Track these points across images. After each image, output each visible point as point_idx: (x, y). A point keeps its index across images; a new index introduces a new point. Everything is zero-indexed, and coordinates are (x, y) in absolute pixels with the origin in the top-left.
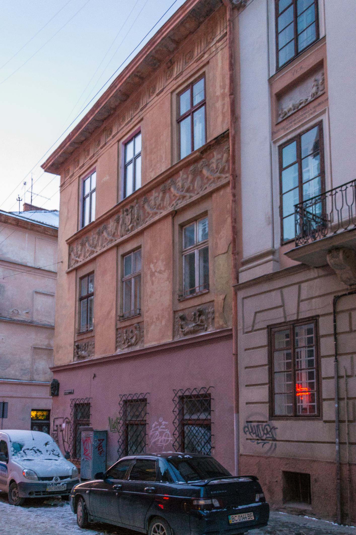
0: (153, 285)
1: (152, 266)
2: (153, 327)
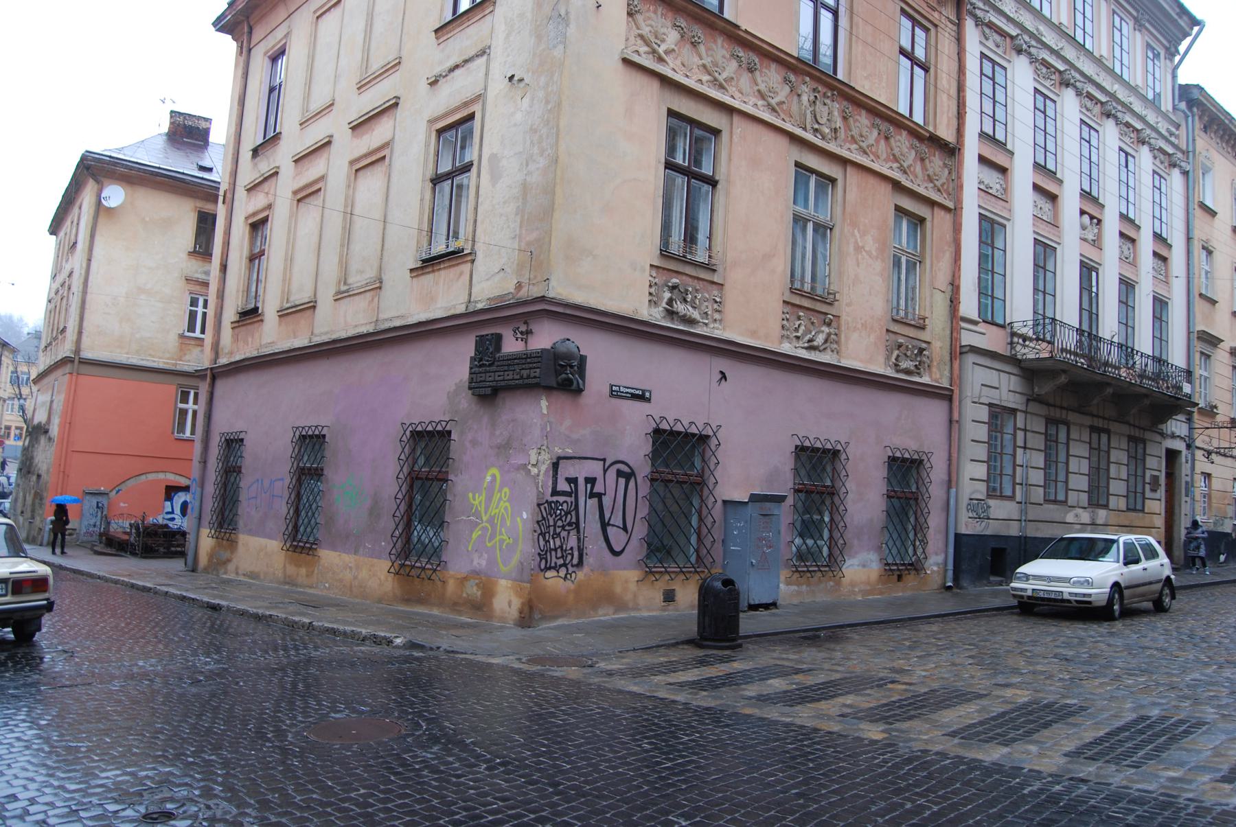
2: (855, 336)
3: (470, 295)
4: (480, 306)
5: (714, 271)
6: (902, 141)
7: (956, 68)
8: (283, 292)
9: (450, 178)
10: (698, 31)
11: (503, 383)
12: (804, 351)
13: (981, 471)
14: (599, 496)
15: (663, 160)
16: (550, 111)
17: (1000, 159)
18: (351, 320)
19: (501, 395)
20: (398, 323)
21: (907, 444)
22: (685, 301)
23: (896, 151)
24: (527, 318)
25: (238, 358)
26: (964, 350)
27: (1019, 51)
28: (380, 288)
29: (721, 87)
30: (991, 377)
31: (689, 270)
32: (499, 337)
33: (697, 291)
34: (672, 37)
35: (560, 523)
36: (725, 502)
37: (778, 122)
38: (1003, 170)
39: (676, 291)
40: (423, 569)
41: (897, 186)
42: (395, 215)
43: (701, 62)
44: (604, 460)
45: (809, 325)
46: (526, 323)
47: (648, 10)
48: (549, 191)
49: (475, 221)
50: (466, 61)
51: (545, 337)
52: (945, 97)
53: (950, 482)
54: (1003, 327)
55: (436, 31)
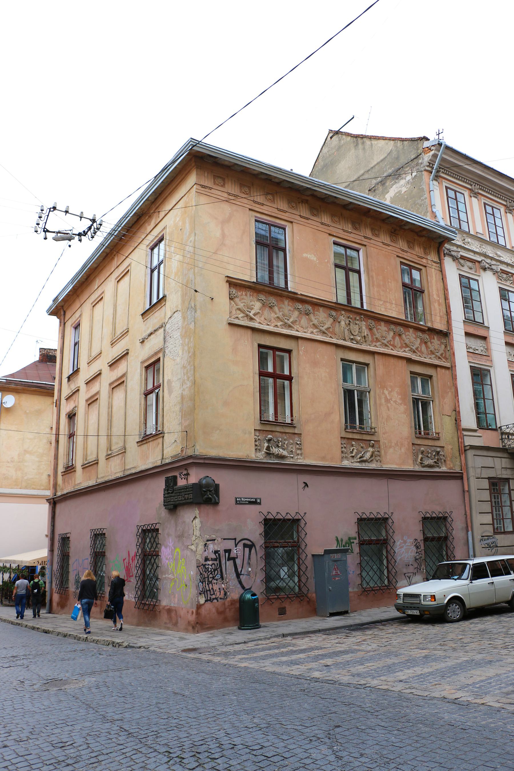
0: (389, 410)
1: (386, 392)
2: (391, 450)
3: (163, 455)
4: (167, 461)
5: (295, 427)
6: (410, 336)
7: (442, 287)
8: (84, 455)
9: (152, 391)
10: (272, 300)
11: (178, 502)
12: (358, 464)
13: (488, 519)
14: (234, 559)
15: (258, 372)
16: (190, 357)
17: (481, 332)
18: (110, 470)
19: (179, 509)
20: (133, 471)
21: (435, 509)
22: (278, 446)
23: (407, 341)
24: (186, 467)
25: (65, 492)
26: (467, 448)
27: (485, 269)
28: (125, 452)
29: (290, 326)
30: (489, 462)
31: (278, 429)
32: (175, 478)
33: (285, 440)
34: (257, 305)
35: (211, 576)
36: (313, 555)
37: (327, 339)
38: (484, 338)
39: (272, 442)
40: (149, 605)
41: (409, 360)
42: (130, 412)
43: (276, 316)
44: (235, 539)
45: (360, 449)
46: (186, 469)
47: (242, 295)
48: (193, 399)
49: (163, 415)
50: (155, 331)
51: (195, 477)
52: (436, 305)
53: (468, 527)
54: (496, 430)
55: (142, 315)
